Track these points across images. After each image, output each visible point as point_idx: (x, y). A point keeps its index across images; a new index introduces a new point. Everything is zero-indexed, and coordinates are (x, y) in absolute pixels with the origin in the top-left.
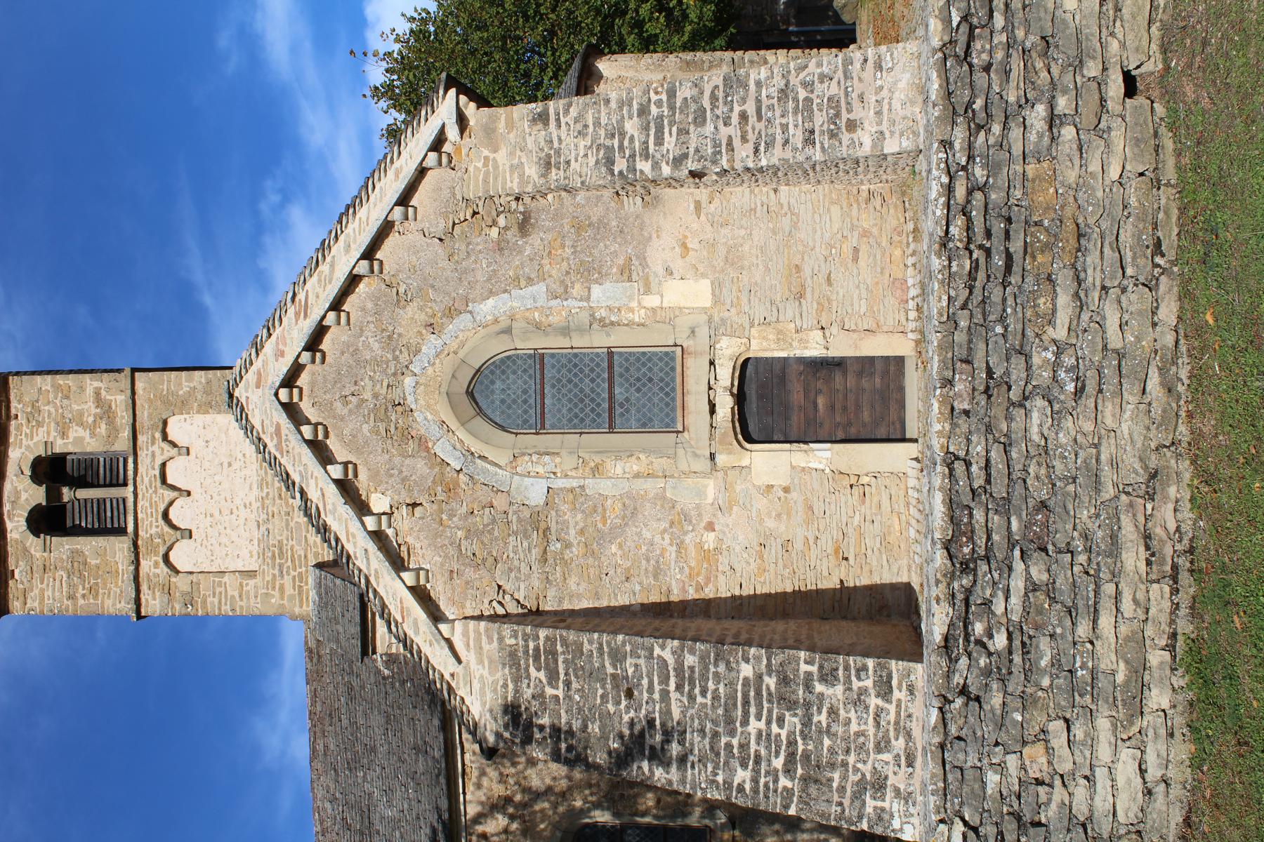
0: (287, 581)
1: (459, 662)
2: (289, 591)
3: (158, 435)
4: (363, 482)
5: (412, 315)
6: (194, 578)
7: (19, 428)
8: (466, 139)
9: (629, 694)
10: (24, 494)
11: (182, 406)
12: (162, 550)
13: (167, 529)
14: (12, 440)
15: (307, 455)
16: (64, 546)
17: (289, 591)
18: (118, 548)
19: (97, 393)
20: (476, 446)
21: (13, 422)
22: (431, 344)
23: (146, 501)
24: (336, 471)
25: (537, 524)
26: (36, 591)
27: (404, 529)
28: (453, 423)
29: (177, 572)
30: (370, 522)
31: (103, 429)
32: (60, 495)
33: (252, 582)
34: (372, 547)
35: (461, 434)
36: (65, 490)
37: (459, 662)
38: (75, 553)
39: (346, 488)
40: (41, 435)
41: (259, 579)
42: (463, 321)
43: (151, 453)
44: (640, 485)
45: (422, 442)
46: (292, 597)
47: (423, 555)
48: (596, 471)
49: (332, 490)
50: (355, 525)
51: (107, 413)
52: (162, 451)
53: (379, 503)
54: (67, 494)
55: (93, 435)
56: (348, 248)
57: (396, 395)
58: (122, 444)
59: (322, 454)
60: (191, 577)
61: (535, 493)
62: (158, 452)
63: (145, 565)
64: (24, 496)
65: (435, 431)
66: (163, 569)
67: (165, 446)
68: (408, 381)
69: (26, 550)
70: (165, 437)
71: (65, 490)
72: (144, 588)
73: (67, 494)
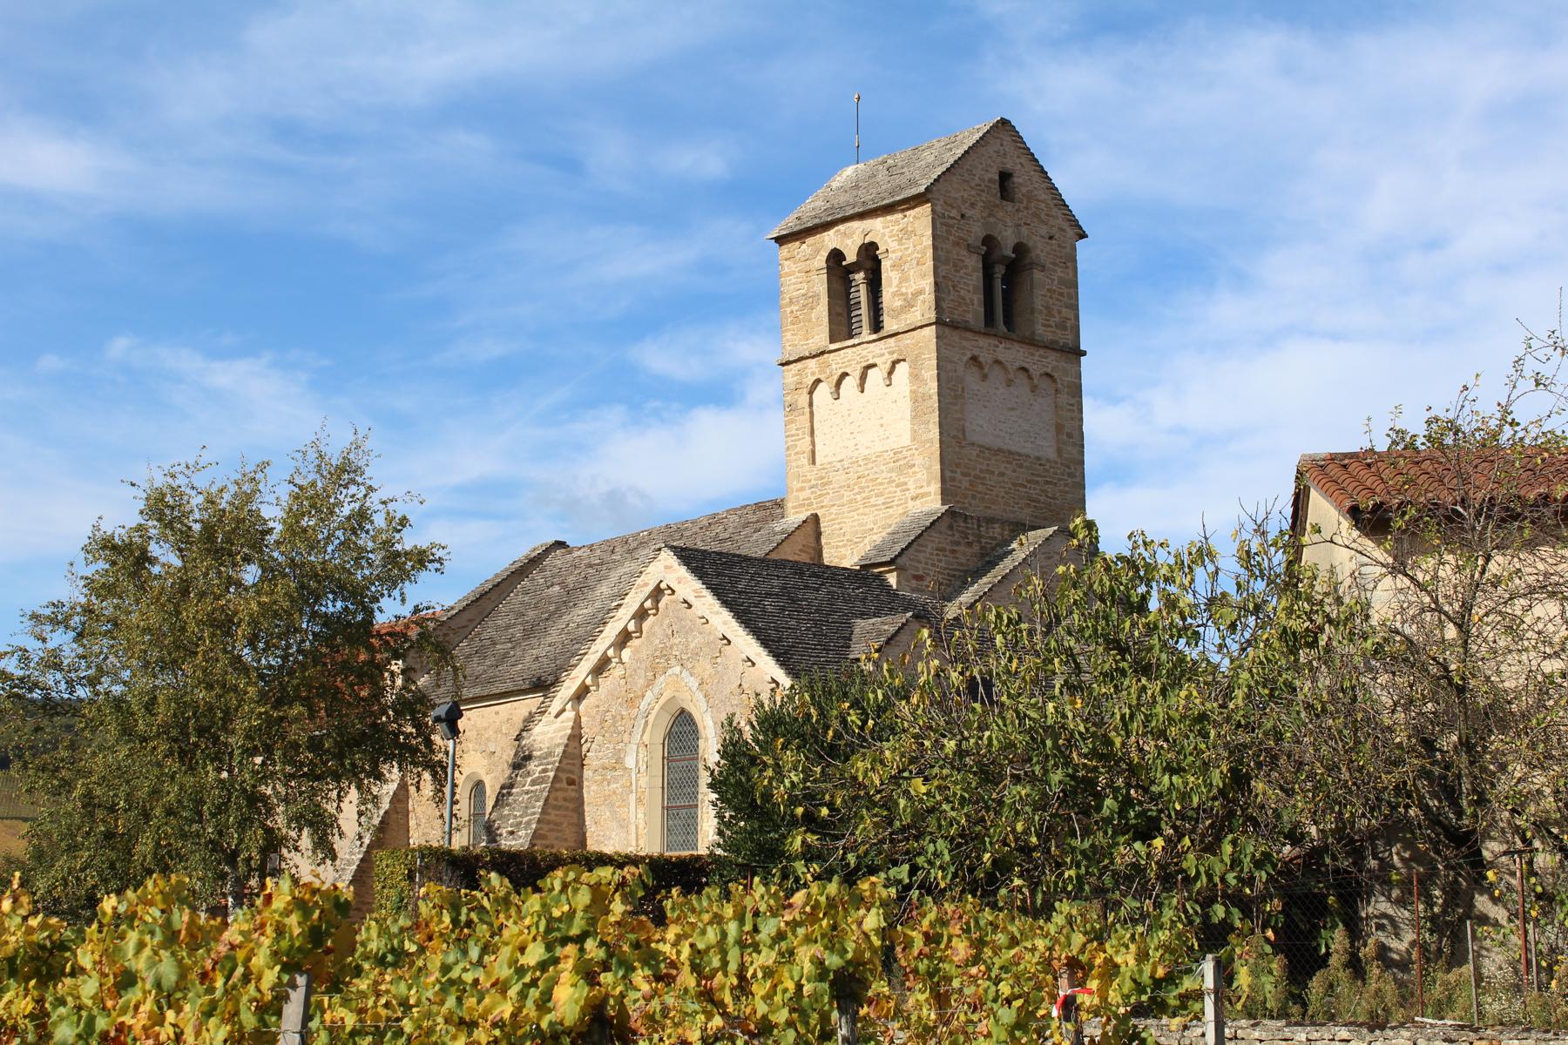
0: (807, 493)
1: (557, 716)
2: (802, 495)
3: (895, 357)
4: (634, 643)
5: (705, 667)
6: (807, 410)
7: (897, 222)
8: (731, 710)
9: (512, 833)
10: (848, 239)
11: (915, 377)
12: (822, 377)
13: (836, 378)
14: (889, 218)
15: (636, 606)
16: (820, 284)
17: (802, 495)
18: (820, 338)
19: (921, 292)
20: (651, 718)
21: (900, 215)
22: (693, 683)
23: (849, 357)
24: (631, 627)
25: (620, 761)
26: (793, 268)
27: (616, 671)
28: (662, 701)
29: (811, 393)
30: (611, 653)
31: (898, 303)
32: (858, 271)
33: (805, 461)
34: (599, 655)
35: (657, 707)
36: (862, 275)
37: (557, 716)
38: (816, 296)
39: (624, 638)
40: (893, 245)
41: (807, 467)
42: (703, 704)
43: (880, 352)
44: (633, 828)
45: (650, 684)
46: (797, 498)
47: (607, 683)
48: (639, 800)
49: (619, 626)
50: (608, 643)
51: (909, 305)
52: (884, 364)
53: (626, 654)
54: (859, 277)
55: (894, 294)
56: (725, 623)
57: (673, 662)
58: (890, 325)
59: (641, 615)
60: (806, 405)
61: (630, 762)
62: (883, 359)
63: (812, 363)
64: (849, 242)
65: (656, 690)
66: (810, 380)
67: (889, 365)
68: (677, 669)
69: (818, 251)
70: (894, 363)
71: (862, 275)
72: (799, 365)
73: (859, 277)
